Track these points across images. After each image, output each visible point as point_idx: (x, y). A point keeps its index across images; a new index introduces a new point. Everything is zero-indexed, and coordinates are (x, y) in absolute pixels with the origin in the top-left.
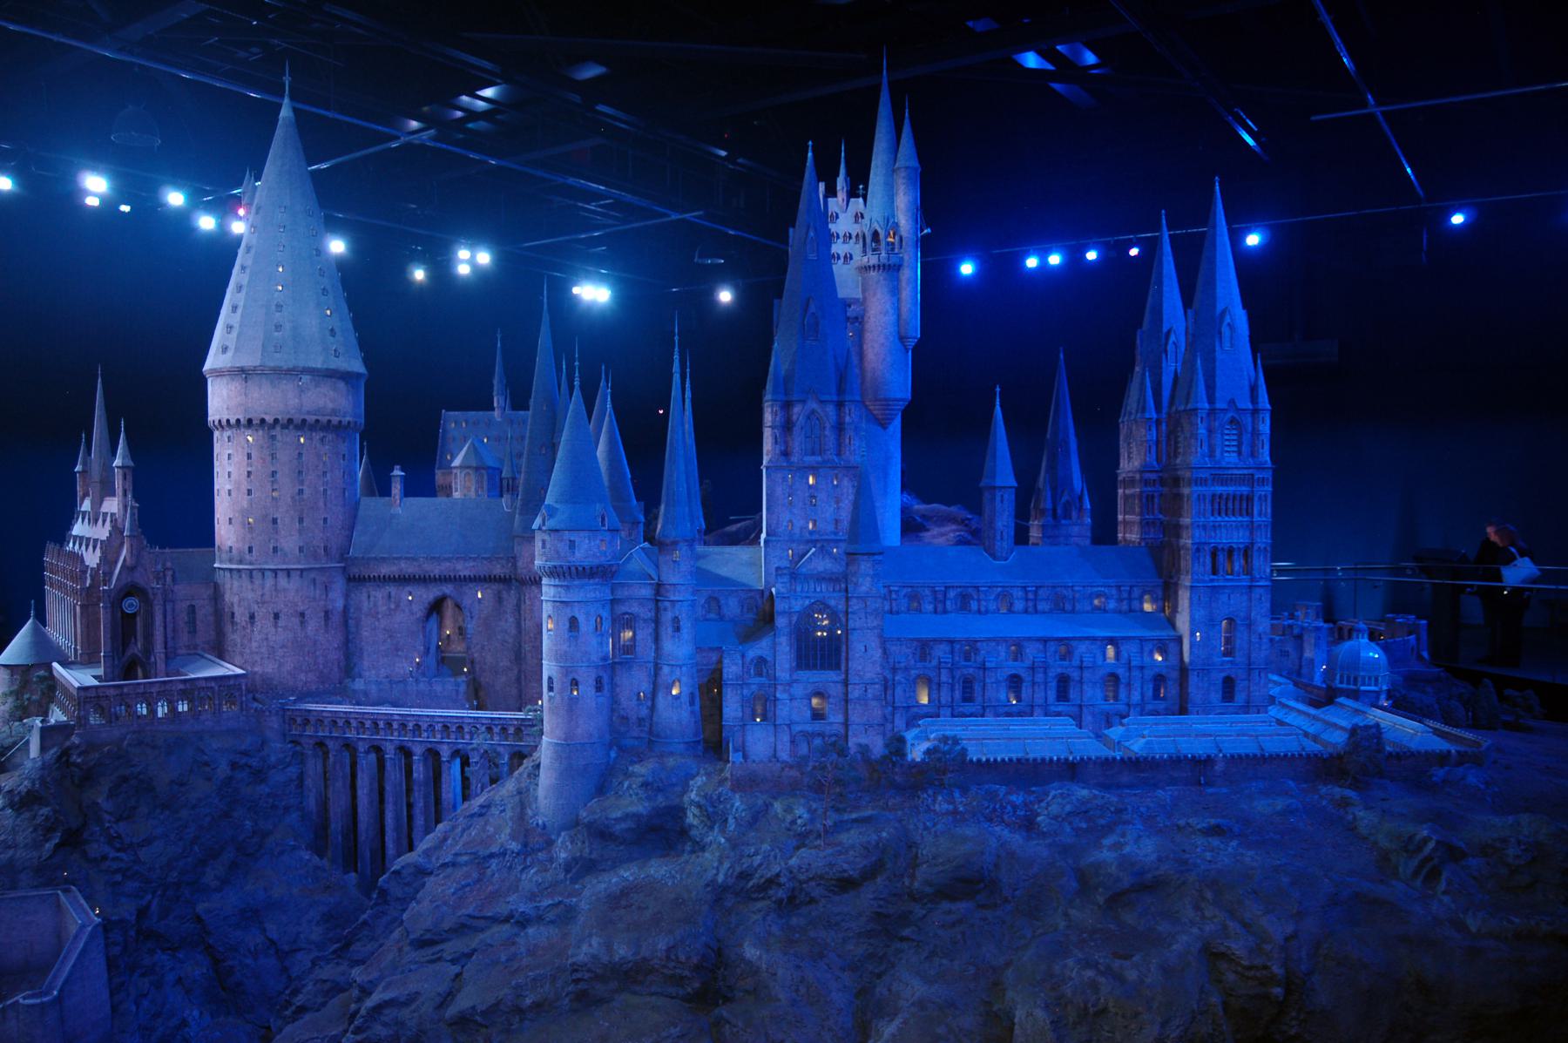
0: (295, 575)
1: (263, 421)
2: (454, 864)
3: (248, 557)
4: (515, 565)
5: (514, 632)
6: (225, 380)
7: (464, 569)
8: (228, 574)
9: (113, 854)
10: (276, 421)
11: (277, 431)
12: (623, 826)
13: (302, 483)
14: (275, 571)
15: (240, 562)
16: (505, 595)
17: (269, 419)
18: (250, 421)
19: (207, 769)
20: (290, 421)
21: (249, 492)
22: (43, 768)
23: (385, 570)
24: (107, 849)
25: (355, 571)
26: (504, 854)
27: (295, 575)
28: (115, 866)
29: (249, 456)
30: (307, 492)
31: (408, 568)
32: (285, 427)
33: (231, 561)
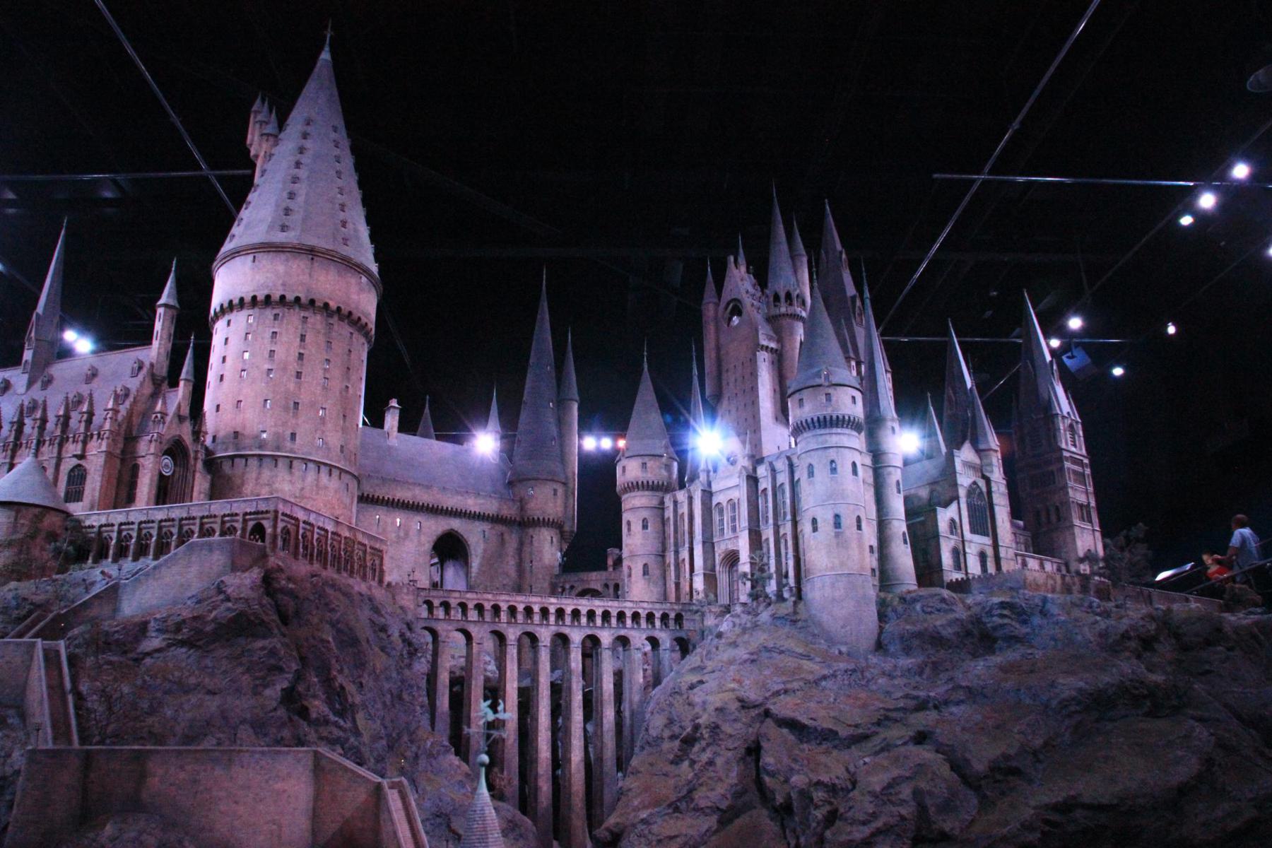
0: (335, 473)
1: (326, 305)
2: (786, 692)
3: (288, 444)
4: (522, 509)
5: (513, 574)
6: (283, 256)
7: (472, 504)
8: (253, 463)
9: (332, 718)
10: (339, 309)
11: (335, 320)
12: (950, 630)
13: (349, 379)
14: (319, 464)
15: (278, 449)
16: (506, 537)
17: (333, 305)
18: (312, 302)
19: (383, 635)
20: (350, 313)
21: (299, 375)
22: (252, 588)
23: (402, 494)
24: (325, 709)
25: (368, 489)
26: (834, 676)
27: (335, 473)
28: (337, 733)
29: (303, 338)
30: (351, 391)
31: (424, 497)
32: (341, 319)
33: (260, 447)
